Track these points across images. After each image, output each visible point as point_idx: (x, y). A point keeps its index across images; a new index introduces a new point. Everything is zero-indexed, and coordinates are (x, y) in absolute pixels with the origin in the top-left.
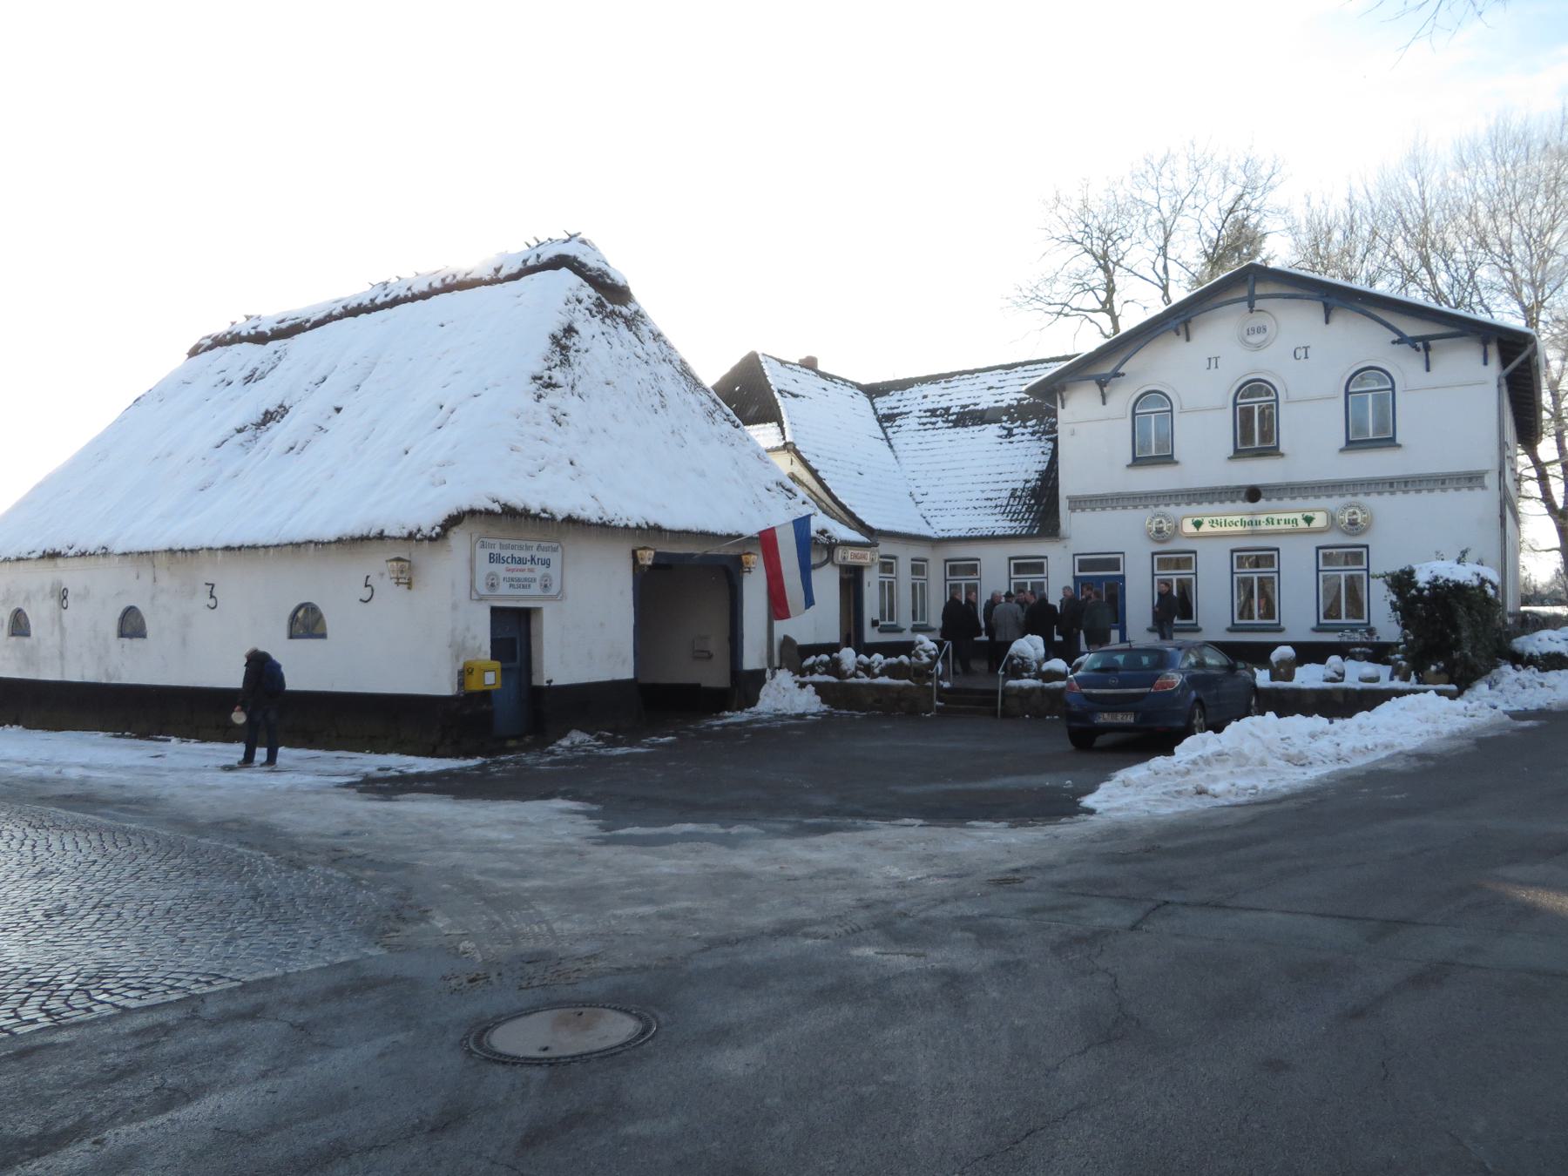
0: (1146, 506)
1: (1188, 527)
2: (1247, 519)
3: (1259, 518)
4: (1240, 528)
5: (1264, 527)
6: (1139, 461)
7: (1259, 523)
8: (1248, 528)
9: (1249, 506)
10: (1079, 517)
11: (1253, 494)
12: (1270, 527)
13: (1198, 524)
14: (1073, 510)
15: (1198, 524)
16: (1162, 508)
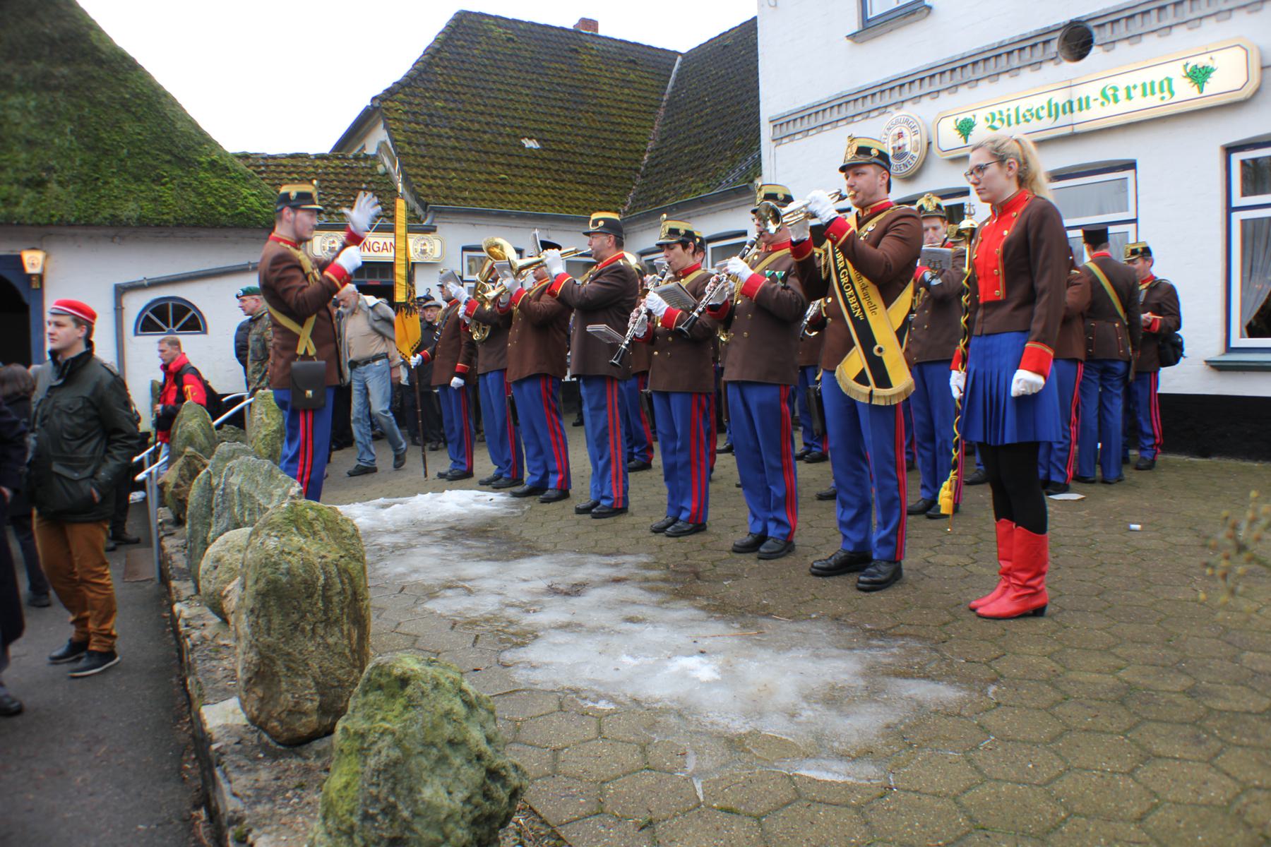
0: (883, 109)
1: (949, 137)
2: (1060, 98)
3: (1080, 92)
4: (1047, 122)
5: (1097, 114)
6: (870, 27)
7: (1084, 104)
8: (1064, 119)
9: (1069, 68)
10: (787, 148)
11: (1077, 40)
12: (1112, 109)
13: (965, 128)
14: (777, 140)
15: (965, 128)
16: (909, 110)
